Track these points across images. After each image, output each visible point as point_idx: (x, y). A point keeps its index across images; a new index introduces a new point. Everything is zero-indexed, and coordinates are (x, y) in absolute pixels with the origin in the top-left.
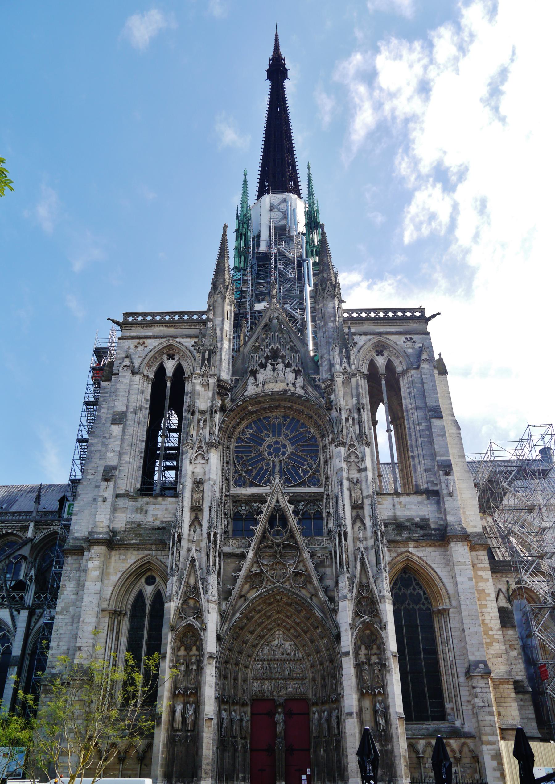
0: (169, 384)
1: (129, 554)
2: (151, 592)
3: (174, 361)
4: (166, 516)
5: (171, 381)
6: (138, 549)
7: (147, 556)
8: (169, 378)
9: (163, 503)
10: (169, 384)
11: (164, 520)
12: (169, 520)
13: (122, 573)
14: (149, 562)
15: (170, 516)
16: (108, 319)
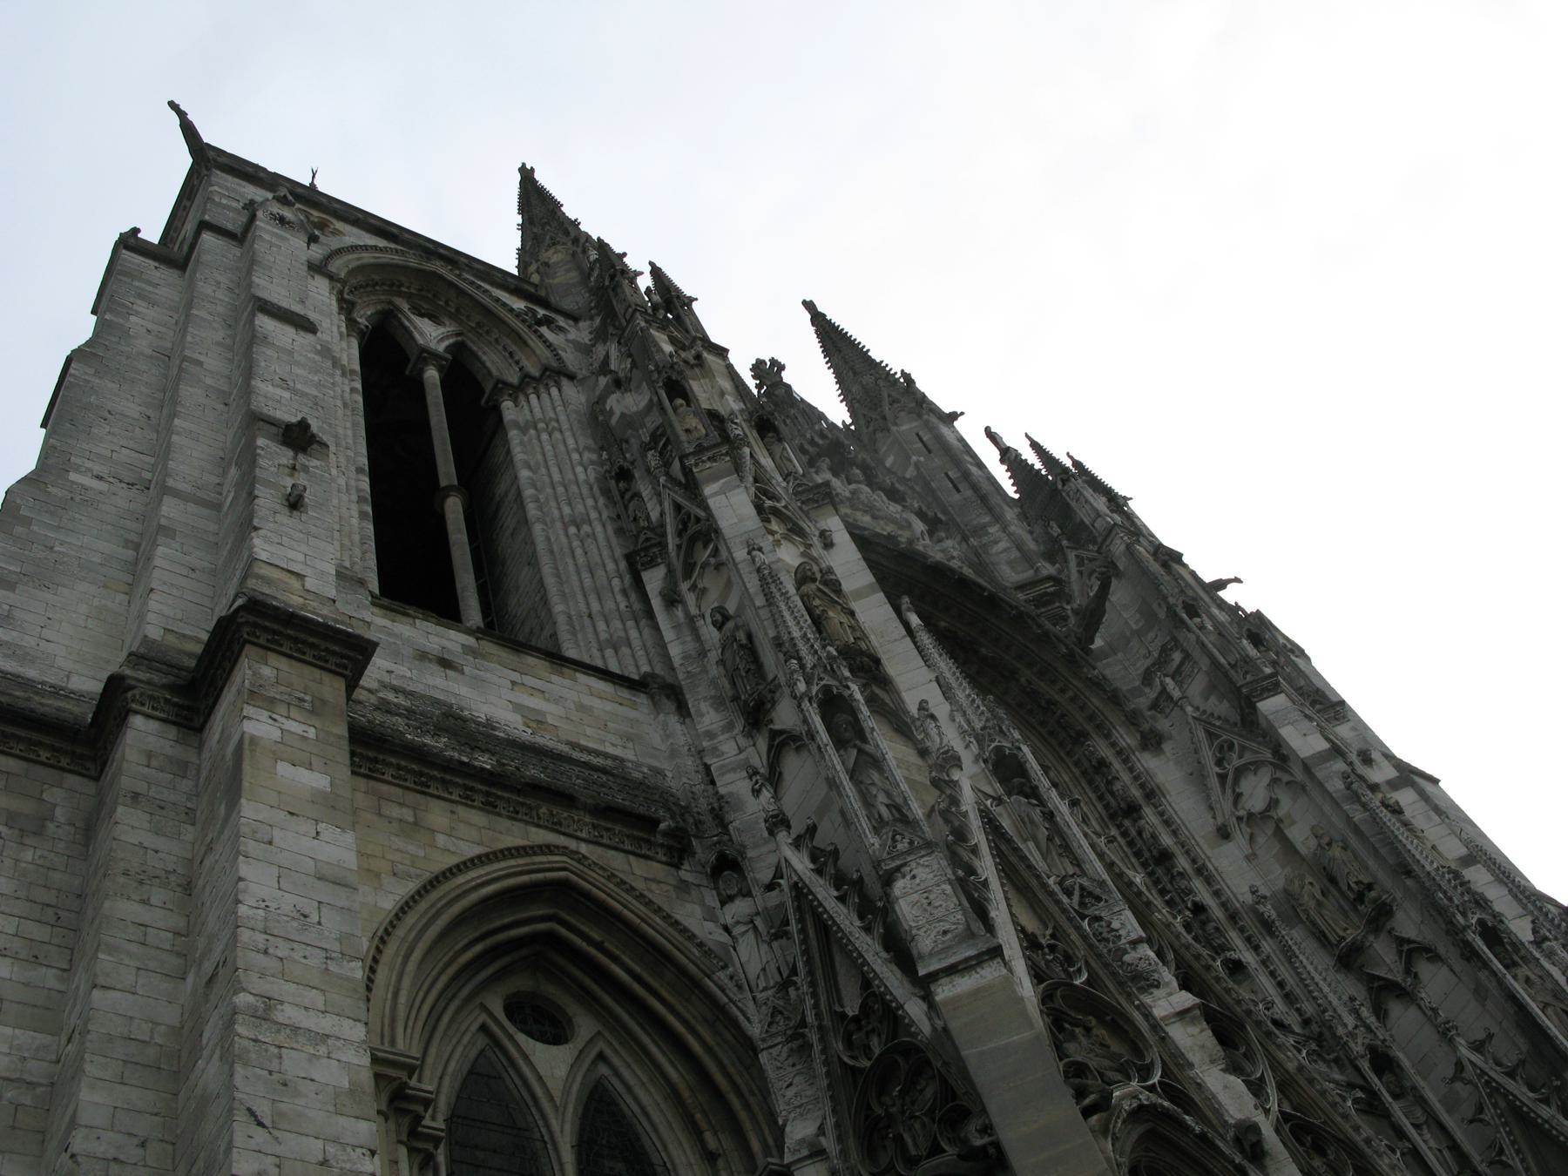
0: (432, 375)
1: (437, 814)
2: (561, 1071)
3: (442, 330)
4: (589, 731)
5: (440, 369)
6: (489, 806)
7: (548, 849)
8: (434, 355)
9: (555, 678)
10: (432, 375)
11: (583, 742)
12: (610, 750)
13: (412, 886)
14: (563, 886)
15: (614, 739)
16: (173, 105)
